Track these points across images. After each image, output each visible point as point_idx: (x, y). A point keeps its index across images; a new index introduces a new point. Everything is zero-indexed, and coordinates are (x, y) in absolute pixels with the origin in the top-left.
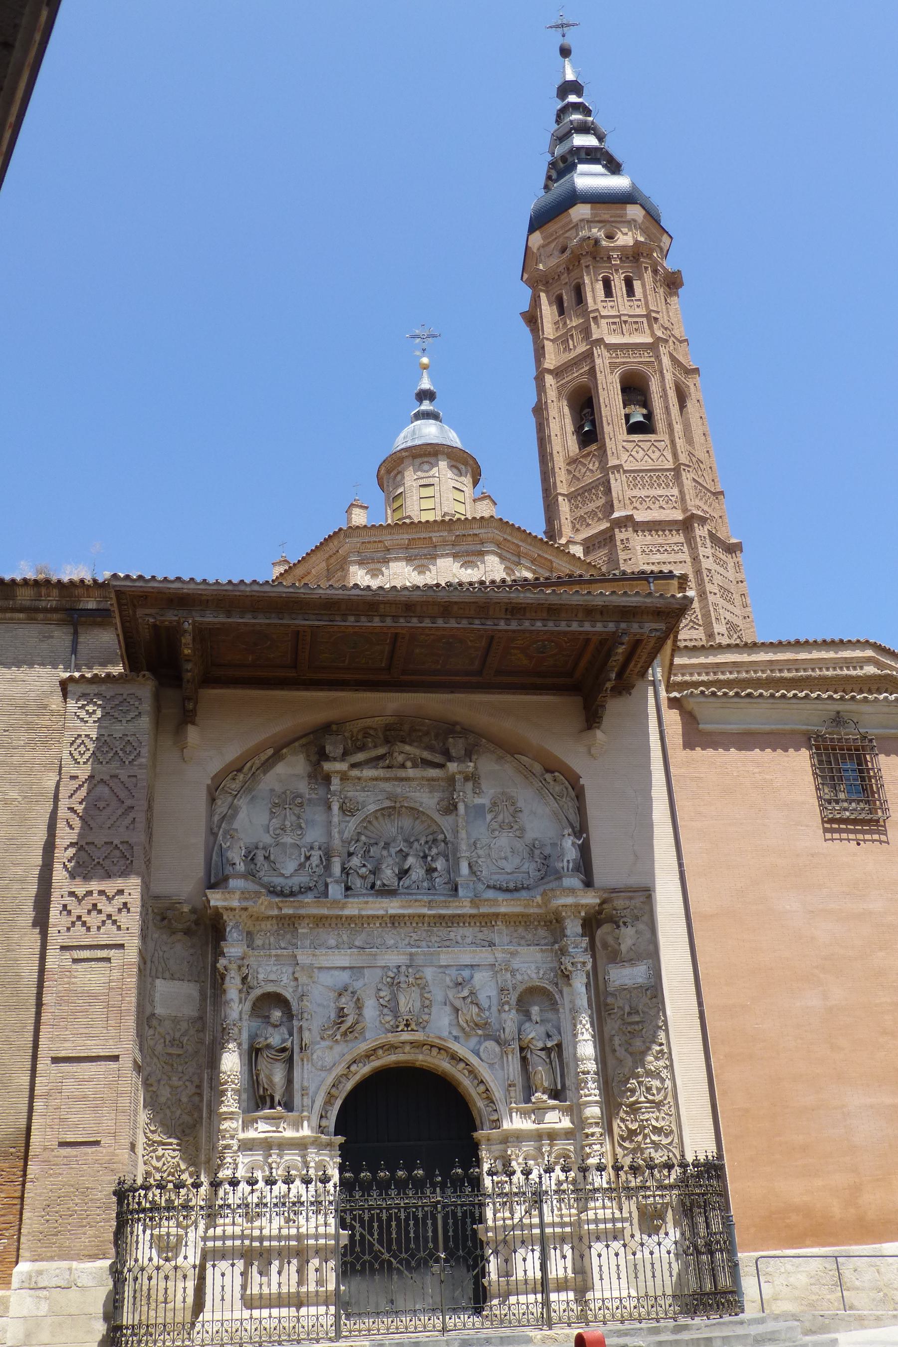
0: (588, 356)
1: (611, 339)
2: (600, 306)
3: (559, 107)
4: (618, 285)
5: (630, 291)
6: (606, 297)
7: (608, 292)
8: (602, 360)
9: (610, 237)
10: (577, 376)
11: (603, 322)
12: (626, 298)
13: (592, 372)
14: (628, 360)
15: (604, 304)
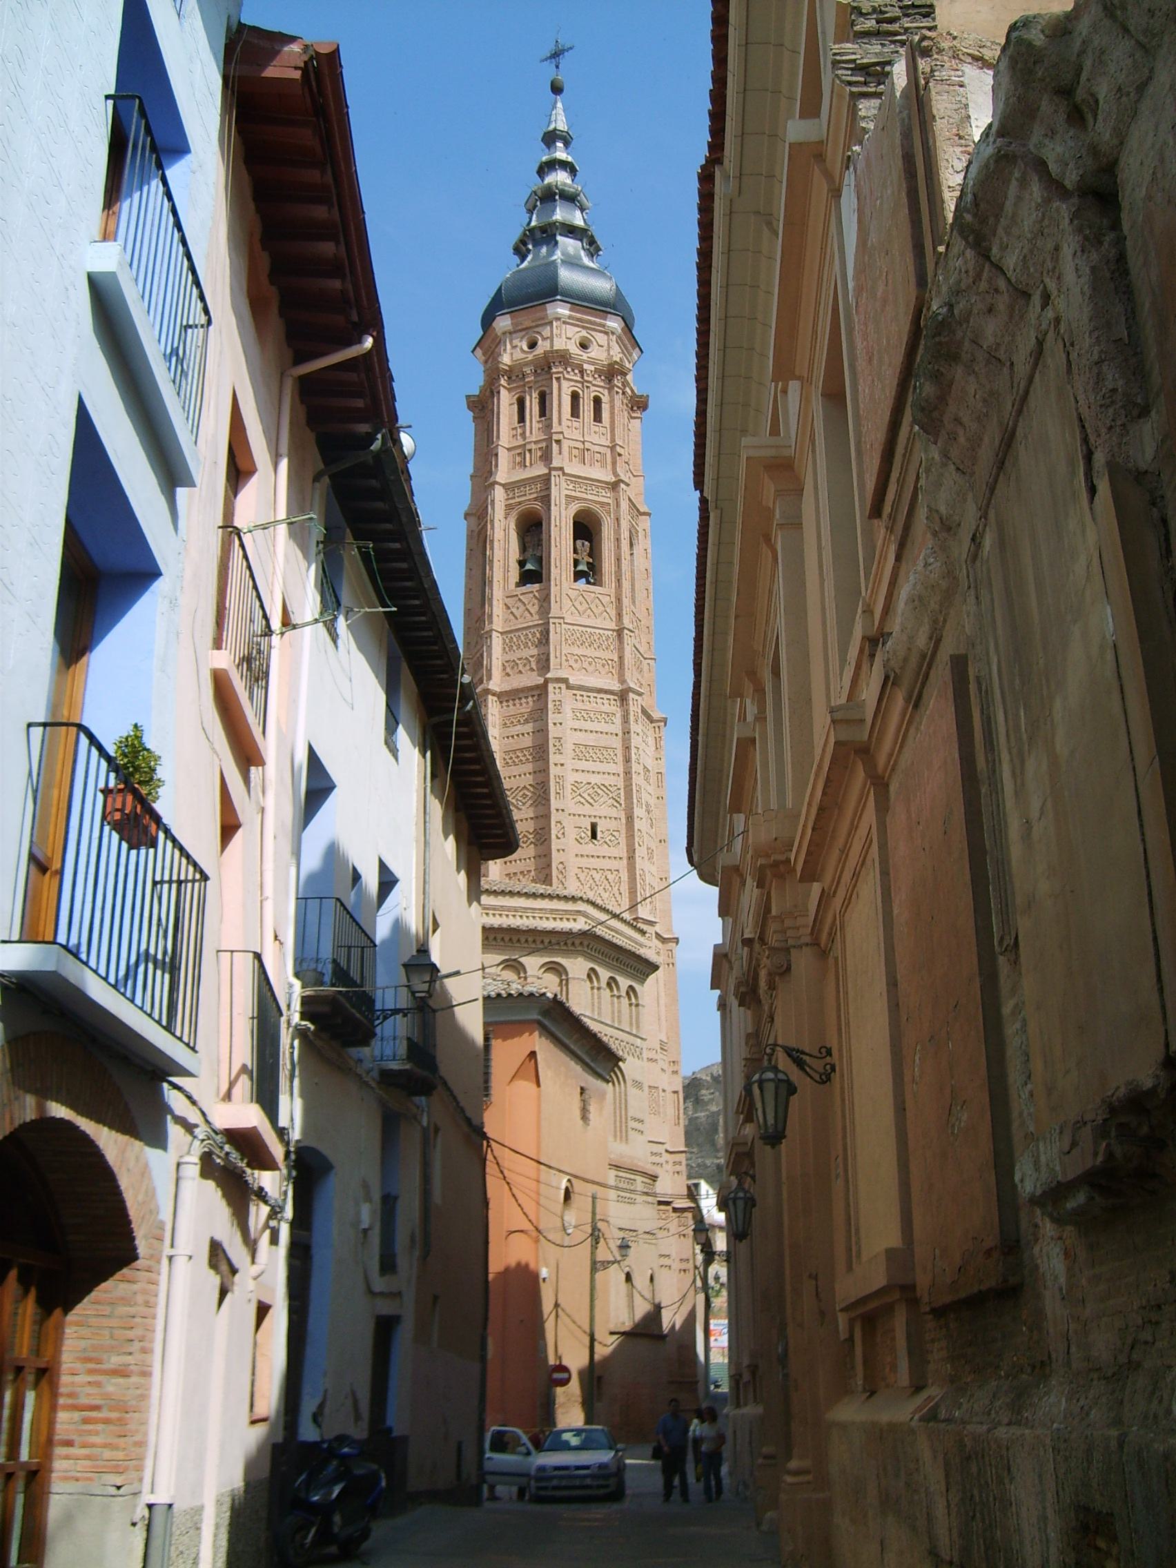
0: (546, 480)
1: (573, 468)
2: (564, 428)
3: (544, 159)
4: (587, 408)
5: (598, 417)
6: (572, 416)
7: (575, 412)
8: (560, 488)
9: (584, 346)
10: (528, 498)
11: (565, 444)
12: (592, 423)
13: (546, 499)
14: (585, 496)
15: (569, 423)
